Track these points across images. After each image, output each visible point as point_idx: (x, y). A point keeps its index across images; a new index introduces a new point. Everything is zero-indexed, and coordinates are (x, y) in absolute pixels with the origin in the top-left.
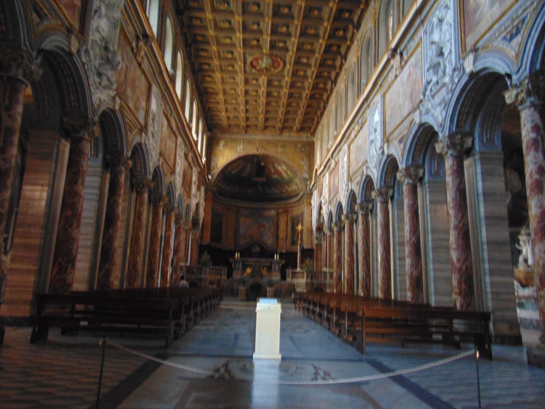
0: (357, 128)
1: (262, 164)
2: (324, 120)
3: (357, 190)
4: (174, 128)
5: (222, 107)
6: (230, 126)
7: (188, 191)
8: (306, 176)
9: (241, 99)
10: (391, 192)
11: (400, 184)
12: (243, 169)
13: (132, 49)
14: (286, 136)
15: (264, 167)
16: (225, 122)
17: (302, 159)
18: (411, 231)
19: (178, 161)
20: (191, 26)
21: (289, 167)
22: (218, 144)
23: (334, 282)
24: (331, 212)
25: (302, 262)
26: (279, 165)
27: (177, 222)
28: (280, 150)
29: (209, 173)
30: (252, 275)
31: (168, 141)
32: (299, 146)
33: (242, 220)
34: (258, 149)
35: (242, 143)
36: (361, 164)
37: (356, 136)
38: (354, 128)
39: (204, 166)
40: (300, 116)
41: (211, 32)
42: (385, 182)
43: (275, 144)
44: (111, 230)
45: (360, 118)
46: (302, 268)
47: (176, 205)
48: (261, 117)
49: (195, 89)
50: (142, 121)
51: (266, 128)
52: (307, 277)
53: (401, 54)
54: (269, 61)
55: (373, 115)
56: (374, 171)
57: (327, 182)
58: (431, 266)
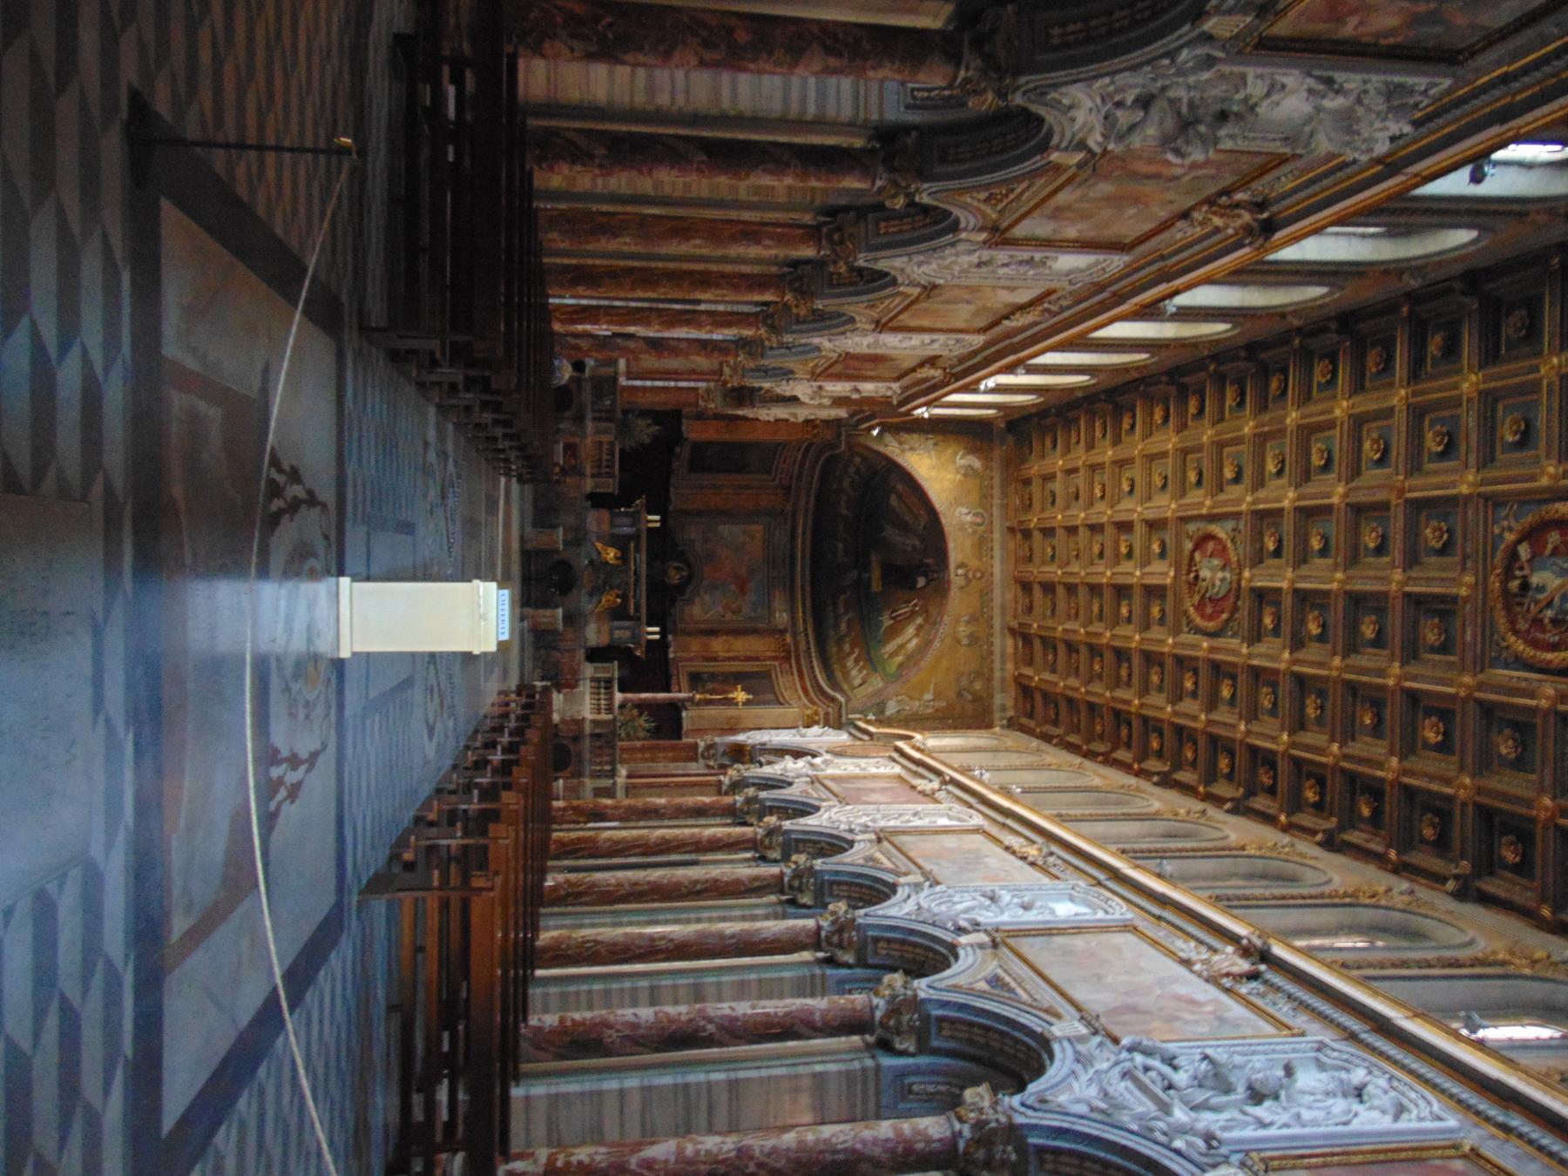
0: (1032, 852)
1: (921, 582)
2: (1055, 755)
3: (851, 860)
4: (1007, 324)
5: (1080, 457)
6: (1027, 482)
7: (832, 370)
8: (892, 708)
9: (1103, 513)
10: (849, 958)
11: (872, 985)
12: (904, 527)
13: (1227, 192)
14: (1004, 645)
15: (913, 586)
16: (1035, 468)
18: (733, 1019)
19: (916, 339)
20: (1307, 358)
21: (913, 658)
22: (972, 450)
23: (587, 799)
24: (790, 784)
25: (641, 706)
26: (919, 628)
27: (741, 344)
28: (963, 630)
29: (886, 428)
30: (598, 565)
31: (972, 307)
32: (978, 686)
33: (757, 529)
34: (959, 567)
35: (979, 520)
36: (927, 866)
37: (1007, 848)
38: (1033, 842)
39: (908, 413)
40: (1065, 683)
41: (1293, 417)
42: (876, 940)
43: (980, 617)
44: (704, 158)
45: (1059, 857)
46: (622, 706)
47: (788, 338)
48: (1054, 572)
49: (1128, 378)
50: (1019, 231)
51: (1026, 587)
52: (595, 723)
53: (1253, 976)
54: (1219, 589)
55: (1072, 899)
56: (910, 906)
57: (873, 770)
58: (632, 1082)
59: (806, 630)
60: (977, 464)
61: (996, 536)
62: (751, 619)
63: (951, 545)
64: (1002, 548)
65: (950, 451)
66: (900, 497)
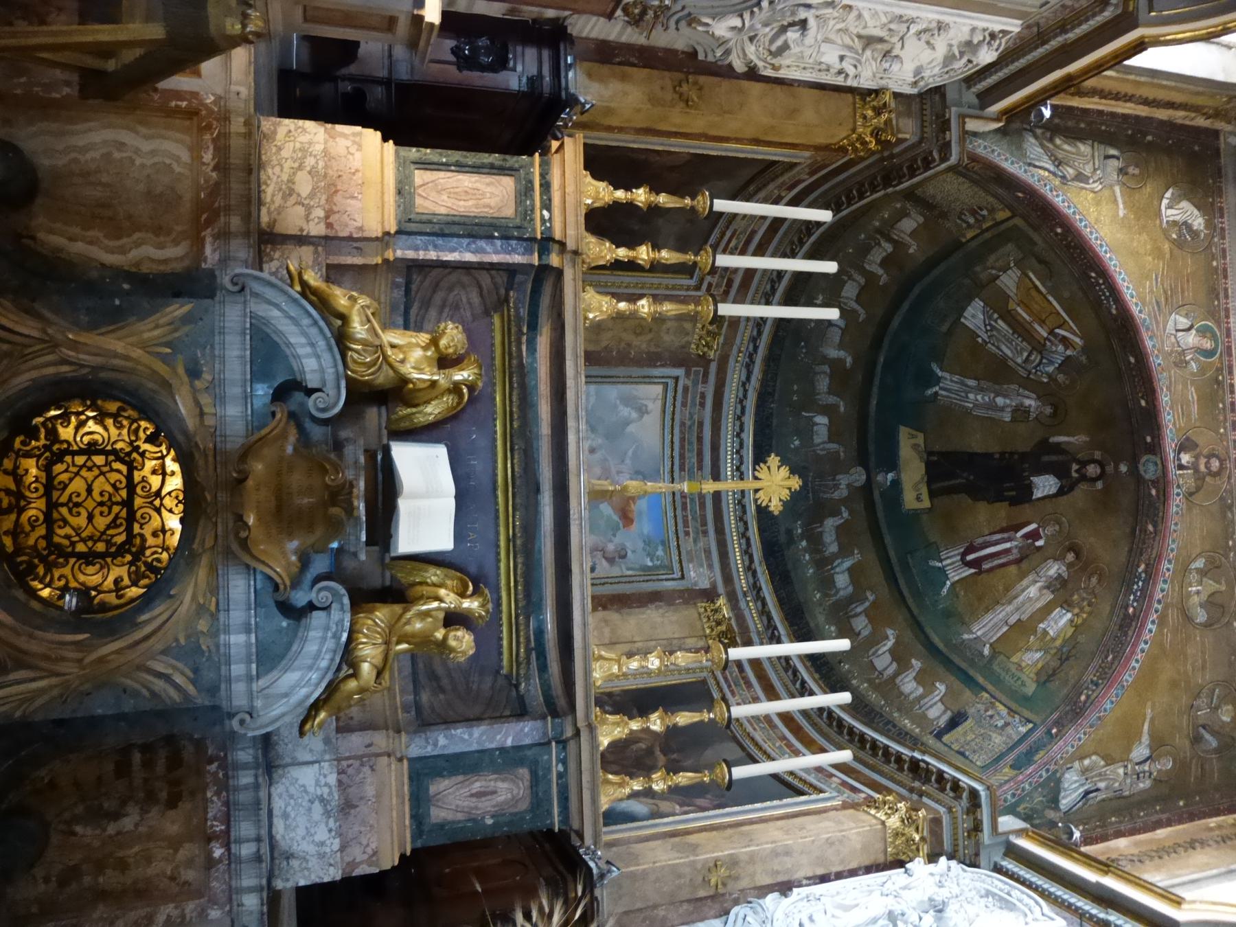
1: (1045, 485)
8: (1072, 791)
15: (1024, 494)
17: (1158, 744)
28: (1198, 591)
34: (1182, 448)
35: (1208, 344)
59: (756, 588)
60: (1198, 222)
62: (645, 569)
63: (1164, 399)
65: (1148, 189)
66: (999, 306)
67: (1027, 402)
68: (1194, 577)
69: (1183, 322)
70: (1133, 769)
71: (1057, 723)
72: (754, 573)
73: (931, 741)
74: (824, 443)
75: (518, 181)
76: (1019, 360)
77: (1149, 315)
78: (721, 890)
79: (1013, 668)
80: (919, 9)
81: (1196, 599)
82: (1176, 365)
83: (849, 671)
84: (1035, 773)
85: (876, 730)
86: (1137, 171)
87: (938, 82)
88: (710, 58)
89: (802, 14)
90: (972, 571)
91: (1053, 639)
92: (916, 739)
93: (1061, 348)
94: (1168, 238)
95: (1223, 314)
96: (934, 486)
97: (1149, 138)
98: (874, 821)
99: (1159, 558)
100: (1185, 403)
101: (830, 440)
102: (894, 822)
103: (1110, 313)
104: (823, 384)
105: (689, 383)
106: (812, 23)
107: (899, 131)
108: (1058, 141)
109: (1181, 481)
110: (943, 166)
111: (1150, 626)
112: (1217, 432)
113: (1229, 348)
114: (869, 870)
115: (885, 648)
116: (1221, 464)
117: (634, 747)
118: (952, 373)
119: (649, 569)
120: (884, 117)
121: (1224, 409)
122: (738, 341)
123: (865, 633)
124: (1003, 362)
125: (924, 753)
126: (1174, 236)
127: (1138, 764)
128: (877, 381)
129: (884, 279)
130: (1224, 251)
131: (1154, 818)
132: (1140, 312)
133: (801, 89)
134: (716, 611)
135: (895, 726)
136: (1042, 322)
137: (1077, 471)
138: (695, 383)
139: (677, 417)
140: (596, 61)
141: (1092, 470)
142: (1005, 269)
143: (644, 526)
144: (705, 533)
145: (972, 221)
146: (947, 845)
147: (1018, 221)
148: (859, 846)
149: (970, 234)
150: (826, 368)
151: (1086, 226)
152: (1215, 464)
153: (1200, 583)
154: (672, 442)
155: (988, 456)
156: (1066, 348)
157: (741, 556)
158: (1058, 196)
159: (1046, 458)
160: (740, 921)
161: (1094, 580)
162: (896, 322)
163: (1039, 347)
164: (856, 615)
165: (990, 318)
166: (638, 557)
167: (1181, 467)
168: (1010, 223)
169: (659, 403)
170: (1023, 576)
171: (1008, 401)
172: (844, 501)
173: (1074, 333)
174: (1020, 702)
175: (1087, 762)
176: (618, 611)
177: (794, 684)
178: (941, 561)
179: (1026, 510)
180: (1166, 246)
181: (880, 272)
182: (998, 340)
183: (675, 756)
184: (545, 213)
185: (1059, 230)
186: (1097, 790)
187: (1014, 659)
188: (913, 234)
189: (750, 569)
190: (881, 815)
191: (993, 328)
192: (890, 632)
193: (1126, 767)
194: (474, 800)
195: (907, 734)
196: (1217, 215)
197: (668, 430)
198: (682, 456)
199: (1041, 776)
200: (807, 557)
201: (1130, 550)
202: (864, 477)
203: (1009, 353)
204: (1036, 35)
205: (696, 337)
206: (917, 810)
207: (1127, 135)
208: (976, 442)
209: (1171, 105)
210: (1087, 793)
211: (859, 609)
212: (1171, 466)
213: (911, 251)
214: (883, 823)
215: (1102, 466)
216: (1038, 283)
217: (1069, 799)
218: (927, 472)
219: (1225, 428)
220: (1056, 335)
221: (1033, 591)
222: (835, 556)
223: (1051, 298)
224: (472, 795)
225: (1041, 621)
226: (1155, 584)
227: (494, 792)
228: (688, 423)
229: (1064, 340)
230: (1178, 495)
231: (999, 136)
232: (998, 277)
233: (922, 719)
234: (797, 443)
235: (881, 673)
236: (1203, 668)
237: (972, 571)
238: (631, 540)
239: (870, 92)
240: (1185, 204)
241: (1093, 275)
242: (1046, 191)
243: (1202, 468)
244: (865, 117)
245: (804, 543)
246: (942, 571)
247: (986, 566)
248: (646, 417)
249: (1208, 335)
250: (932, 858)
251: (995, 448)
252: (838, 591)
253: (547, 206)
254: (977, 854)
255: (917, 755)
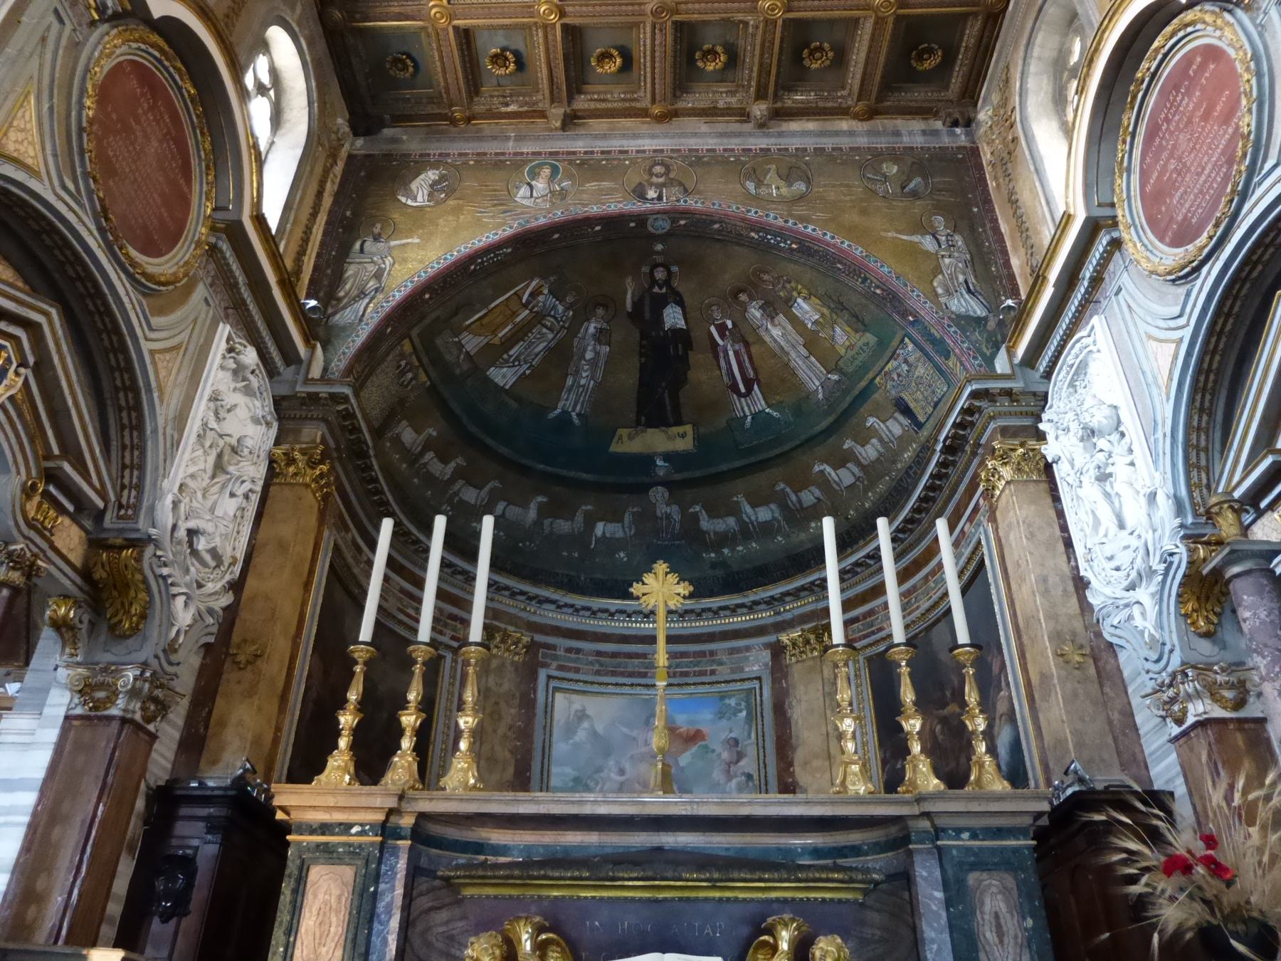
1: (673, 317)
17: (921, 227)
26: (773, 307)
34: (642, 196)
35: (546, 171)
59: (771, 602)
60: (432, 175)
61: (580, 146)
62: (750, 718)
63: (595, 210)
64: (605, 137)
65: (396, 216)
66: (495, 353)
67: (592, 330)
68: (763, 191)
69: (524, 191)
70: (944, 250)
71: (904, 315)
72: (756, 603)
73: (925, 433)
74: (623, 527)
75: (316, 861)
76: (551, 336)
77: (515, 220)
78: (1087, 651)
79: (850, 353)
80: (194, 419)
81: (784, 191)
82: (563, 198)
83: (856, 510)
84: (952, 337)
85: (915, 486)
86: (379, 226)
87: (269, 402)
88: (215, 629)
89: (182, 533)
90: (756, 387)
91: (823, 315)
92: (923, 448)
93: (541, 298)
94: (444, 201)
95: (519, 158)
96: (671, 420)
97: (348, 213)
98: (1007, 491)
99: (743, 220)
100: (601, 191)
101: (621, 520)
102: (1007, 472)
103: (510, 253)
104: (563, 526)
105: (554, 664)
106: (192, 524)
107: (314, 441)
108: (342, 294)
109: (672, 198)
110: (353, 401)
111: (809, 230)
112: (629, 166)
113: (551, 153)
114: (1056, 499)
115: (833, 474)
116: (658, 164)
117: (940, 738)
118: (559, 400)
119: (749, 714)
120: (297, 455)
121: (607, 160)
122: (512, 611)
123: (817, 493)
124: (550, 351)
125: (936, 440)
126: (443, 196)
127: (940, 246)
128: (564, 472)
129: (460, 461)
130: (460, 155)
131: (990, 233)
132: (511, 227)
133: (259, 537)
134: (794, 644)
135: (910, 467)
136: (514, 314)
137: (661, 288)
138: (555, 658)
139: (590, 678)
140: (200, 753)
141: (660, 274)
142: (460, 346)
143: (704, 718)
144: (712, 653)
145: (410, 375)
146: (1027, 422)
147: (415, 333)
148: (1033, 508)
149: (423, 377)
150: (547, 522)
151: (426, 272)
152: (658, 169)
153: (769, 186)
154: (617, 684)
155: (642, 368)
156: (541, 293)
157: (737, 616)
158: (394, 296)
159: (647, 315)
160: (1118, 632)
161: (766, 277)
162: (504, 450)
163: (538, 318)
164: (800, 501)
165: (507, 361)
166: (737, 726)
167: (660, 198)
168: (417, 341)
169: (574, 697)
170: (761, 341)
171: (590, 348)
172: (683, 511)
173: (527, 286)
174: (884, 349)
175: (940, 291)
176: (794, 749)
177: (871, 566)
178: (746, 416)
179: (696, 334)
180: (451, 202)
181: (453, 464)
182: (528, 356)
183: (948, 693)
184: (354, 830)
185: (427, 296)
186: (966, 282)
187: (842, 352)
188: (418, 431)
189: (752, 607)
190: (1001, 484)
191: (517, 359)
192: (817, 468)
193: (943, 256)
194: (1006, 940)
195: (918, 456)
196: (427, 158)
197: (602, 689)
198: (631, 675)
199: (955, 332)
200: (740, 548)
201: (738, 244)
202: (660, 488)
203: (544, 344)
204: (236, 311)
205: (506, 654)
206: (994, 450)
207: (344, 232)
208: (629, 378)
209: (320, 194)
210: (969, 291)
211: (794, 498)
212: (658, 206)
213: (435, 434)
214: (1008, 483)
215: (657, 265)
216: (477, 317)
217: (976, 308)
218: (656, 427)
219: (625, 160)
220: (528, 302)
221: (776, 332)
222: (740, 521)
223: (493, 305)
224: (1001, 942)
225: (805, 325)
226: (770, 225)
227: (997, 916)
228: (597, 667)
229: (533, 295)
230: (685, 201)
231: (330, 347)
232: (467, 353)
233: (903, 441)
234: (622, 555)
235: (858, 479)
236: (847, 186)
237: (756, 387)
238: (718, 732)
239: (271, 468)
240: (414, 186)
241: (472, 267)
242: (388, 307)
243: (661, 180)
244: (296, 474)
245: (726, 551)
246: (755, 416)
247: (751, 374)
248: (588, 712)
249: (537, 170)
250: (1041, 437)
251: (635, 362)
252: (774, 519)
253: (346, 827)
254: (1034, 394)
255: (939, 447)
